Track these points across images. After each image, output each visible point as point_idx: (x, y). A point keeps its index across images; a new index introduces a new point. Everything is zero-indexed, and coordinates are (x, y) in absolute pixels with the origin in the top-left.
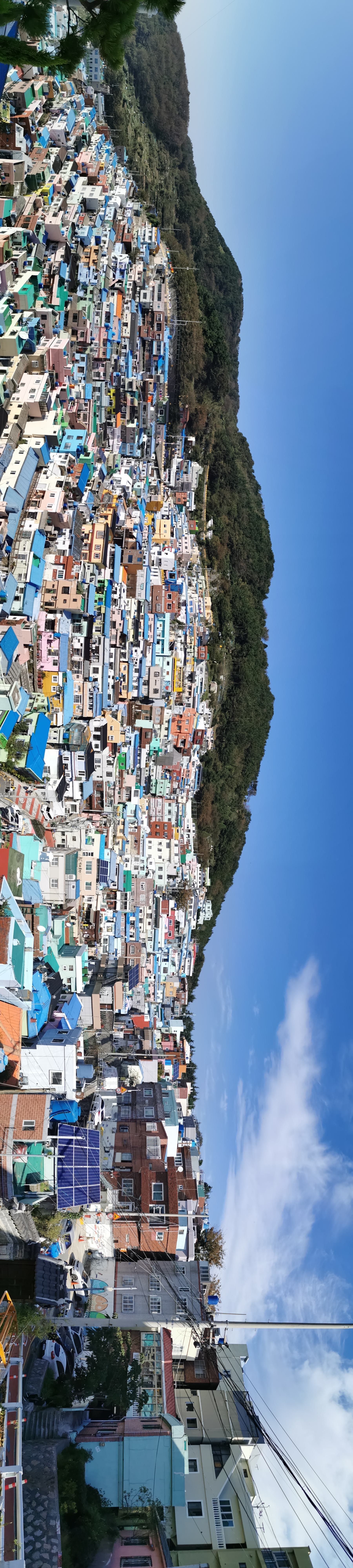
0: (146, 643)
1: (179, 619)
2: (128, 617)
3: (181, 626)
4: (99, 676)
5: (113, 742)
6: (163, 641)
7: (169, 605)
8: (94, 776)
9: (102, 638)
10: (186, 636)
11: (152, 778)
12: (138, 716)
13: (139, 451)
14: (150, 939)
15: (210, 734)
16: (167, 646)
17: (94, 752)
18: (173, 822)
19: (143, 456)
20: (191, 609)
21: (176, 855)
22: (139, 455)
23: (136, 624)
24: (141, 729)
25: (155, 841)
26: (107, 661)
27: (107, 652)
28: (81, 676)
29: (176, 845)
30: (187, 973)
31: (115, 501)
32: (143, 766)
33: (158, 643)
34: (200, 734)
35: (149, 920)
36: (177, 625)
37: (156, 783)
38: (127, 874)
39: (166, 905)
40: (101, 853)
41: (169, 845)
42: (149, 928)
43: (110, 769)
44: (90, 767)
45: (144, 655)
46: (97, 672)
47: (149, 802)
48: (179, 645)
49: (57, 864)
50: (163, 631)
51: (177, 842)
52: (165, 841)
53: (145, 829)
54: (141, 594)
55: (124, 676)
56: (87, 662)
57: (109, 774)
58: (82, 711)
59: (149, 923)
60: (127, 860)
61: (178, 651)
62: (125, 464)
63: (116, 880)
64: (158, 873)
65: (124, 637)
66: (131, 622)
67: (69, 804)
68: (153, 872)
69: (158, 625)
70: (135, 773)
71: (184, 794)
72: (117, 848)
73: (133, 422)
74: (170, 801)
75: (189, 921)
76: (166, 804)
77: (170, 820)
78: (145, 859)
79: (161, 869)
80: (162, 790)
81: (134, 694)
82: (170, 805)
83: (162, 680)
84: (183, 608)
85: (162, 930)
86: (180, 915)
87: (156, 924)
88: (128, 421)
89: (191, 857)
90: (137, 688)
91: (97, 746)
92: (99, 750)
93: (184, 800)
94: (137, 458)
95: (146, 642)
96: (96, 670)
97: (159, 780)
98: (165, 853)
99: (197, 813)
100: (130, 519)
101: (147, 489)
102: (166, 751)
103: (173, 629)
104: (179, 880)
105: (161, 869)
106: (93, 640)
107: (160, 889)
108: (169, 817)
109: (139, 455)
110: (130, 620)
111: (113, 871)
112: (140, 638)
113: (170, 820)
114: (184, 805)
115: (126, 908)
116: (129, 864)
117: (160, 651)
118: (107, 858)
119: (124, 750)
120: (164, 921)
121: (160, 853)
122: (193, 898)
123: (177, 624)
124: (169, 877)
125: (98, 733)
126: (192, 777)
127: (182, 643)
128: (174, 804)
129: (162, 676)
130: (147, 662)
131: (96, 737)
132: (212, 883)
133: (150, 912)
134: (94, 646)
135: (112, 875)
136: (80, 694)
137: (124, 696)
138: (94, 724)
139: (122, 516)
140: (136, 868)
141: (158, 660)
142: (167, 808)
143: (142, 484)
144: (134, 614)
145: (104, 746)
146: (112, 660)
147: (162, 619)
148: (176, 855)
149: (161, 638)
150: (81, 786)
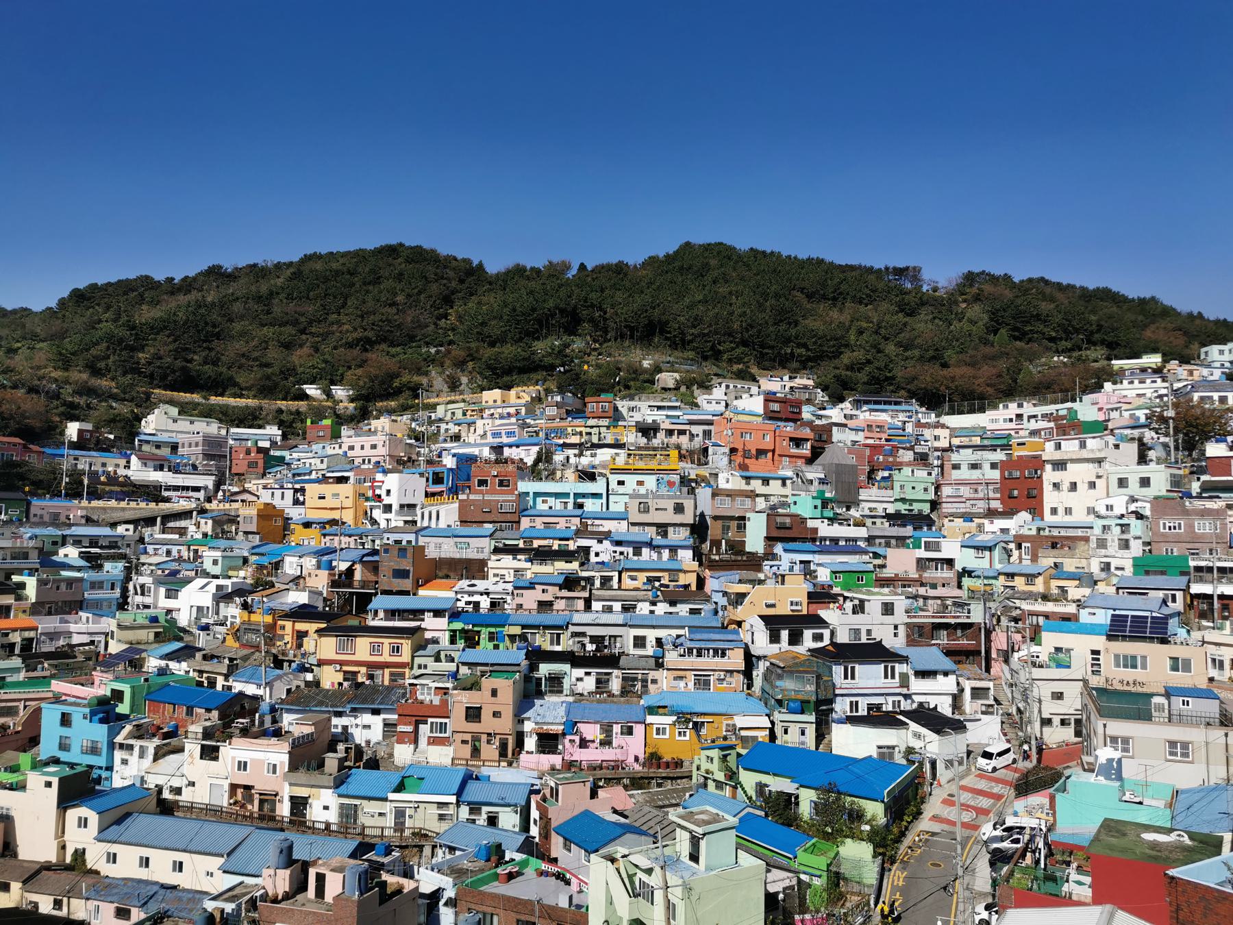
0: (581, 532)
1: (529, 461)
2: (529, 575)
3: (545, 457)
4: (651, 635)
5: (805, 601)
7: (501, 484)
8: (895, 643)
10: (565, 446)
11: (891, 509)
13: (108, 566)
16: (588, 487)
17: (833, 643)
18: (999, 456)
19: (123, 557)
20: (510, 434)
21: (1083, 445)
22: (121, 565)
23: (543, 555)
25: (1050, 498)
26: (619, 618)
27: (600, 618)
28: (652, 675)
29: (1058, 447)
31: (254, 618)
32: (862, 532)
33: (581, 506)
36: (542, 467)
37: (903, 500)
41: (1060, 465)
45: (607, 535)
46: (643, 638)
47: (955, 515)
48: (585, 461)
49: (1126, 741)
50: (557, 495)
51: (1050, 446)
52: (1049, 475)
53: (1021, 523)
54: (478, 547)
58: (731, 672)
61: (596, 461)
62: (148, 600)
64: (1134, 488)
65: (570, 583)
66: (538, 568)
67: (969, 705)
68: (1133, 500)
69: (545, 507)
70: (880, 551)
71: (928, 433)
73: (22, 586)
74: (947, 466)
76: (956, 474)
77: (994, 466)
79: (1122, 483)
80: (920, 487)
81: (686, 556)
82: (956, 467)
84: (507, 452)
88: (19, 598)
90: (673, 550)
91: (818, 638)
92: (826, 633)
94: (128, 570)
95: (579, 533)
96: (640, 642)
97: (897, 493)
100: (305, 576)
101: (223, 543)
103: (551, 476)
104: (1149, 435)
105: (1122, 483)
106: (576, 648)
107: (1176, 482)
108: (987, 466)
109: (121, 565)
112: (572, 546)
113: (994, 466)
117: (598, 502)
119: (823, 575)
123: (541, 466)
124: (1143, 459)
125: (785, 634)
127: (581, 455)
130: (619, 528)
131: (795, 639)
134: (590, 647)
137: (691, 579)
138: (761, 643)
139: (298, 598)
140: (1125, 545)
141: (617, 506)
142: (965, 473)
143: (209, 556)
144: (521, 562)
145: (815, 621)
146: (617, 606)
147: (530, 499)
148: (1083, 445)
149: (571, 500)
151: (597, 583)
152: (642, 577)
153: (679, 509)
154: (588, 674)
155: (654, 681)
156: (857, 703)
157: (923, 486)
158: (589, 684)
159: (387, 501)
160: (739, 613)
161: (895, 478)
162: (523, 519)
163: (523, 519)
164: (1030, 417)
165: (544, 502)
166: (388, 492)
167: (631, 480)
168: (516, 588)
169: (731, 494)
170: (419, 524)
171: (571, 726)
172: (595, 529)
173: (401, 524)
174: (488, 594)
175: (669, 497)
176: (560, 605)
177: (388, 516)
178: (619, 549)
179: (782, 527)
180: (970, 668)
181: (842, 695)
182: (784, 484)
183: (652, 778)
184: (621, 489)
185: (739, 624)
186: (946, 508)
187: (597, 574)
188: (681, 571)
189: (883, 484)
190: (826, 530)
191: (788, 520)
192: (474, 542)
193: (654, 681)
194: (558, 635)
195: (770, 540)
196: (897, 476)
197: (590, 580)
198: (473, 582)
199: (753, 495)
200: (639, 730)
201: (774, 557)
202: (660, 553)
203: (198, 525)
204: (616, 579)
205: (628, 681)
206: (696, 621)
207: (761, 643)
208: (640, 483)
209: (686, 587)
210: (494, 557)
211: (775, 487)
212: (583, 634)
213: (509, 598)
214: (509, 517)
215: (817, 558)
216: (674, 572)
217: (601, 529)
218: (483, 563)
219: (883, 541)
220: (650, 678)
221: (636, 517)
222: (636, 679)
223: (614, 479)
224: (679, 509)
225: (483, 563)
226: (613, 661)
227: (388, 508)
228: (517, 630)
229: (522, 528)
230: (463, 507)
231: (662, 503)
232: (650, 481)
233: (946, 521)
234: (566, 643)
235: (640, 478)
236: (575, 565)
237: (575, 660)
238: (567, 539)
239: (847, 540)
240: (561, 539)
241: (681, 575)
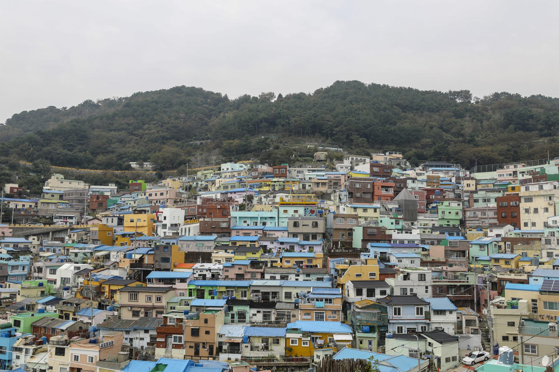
34: (376, 169)
37: (443, 219)
46: (290, 293)
56: (278, 306)
58: (335, 312)
70: (427, 247)
76: (476, 205)
82: (476, 201)
138: (352, 296)
142: (481, 205)
146: (278, 277)
149: (259, 221)
151: (269, 265)
152: (293, 262)
153: (316, 225)
154: (259, 312)
155: (294, 316)
156: (402, 327)
157: (455, 211)
158: (259, 318)
159: (164, 222)
161: (439, 207)
164: (520, 173)
165: (245, 222)
166: (165, 218)
167: (291, 210)
169: (344, 217)
170: (180, 234)
173: (171, 234)
177: (164, 230)
178: (282, 246)
181: (393, 323)
184: (285, 215)
186: (468, 224)
189: (433, 211)
191: (375, 231)
192: (206, 244)
193: (294, 316)
194: (245, 292)
195: (365, 241)
196: (441, 208)
197: (265, 263)
198: (203, 264)
199: (356, 217)
200: (282, 342)
201: (367, 250)
203: (70, 236)
205: (280, 315)
207: (352, 296)
208: (296, 211)
210: (215, 251)
212: (258, 291)
214: (225, 231)
215: (389, 251)
217: (274, 236)
219: (429, 241)
220: (292, 314)
223: (282, 209)
226: (272, 305)
227: (164, 226)
230: (202, 225)
231: (306, 222)
232: (301, 210)
233: (467, 230)
234: (250, 296)
235: (296, 209)
236: (257, 256)
237: (252, 304)
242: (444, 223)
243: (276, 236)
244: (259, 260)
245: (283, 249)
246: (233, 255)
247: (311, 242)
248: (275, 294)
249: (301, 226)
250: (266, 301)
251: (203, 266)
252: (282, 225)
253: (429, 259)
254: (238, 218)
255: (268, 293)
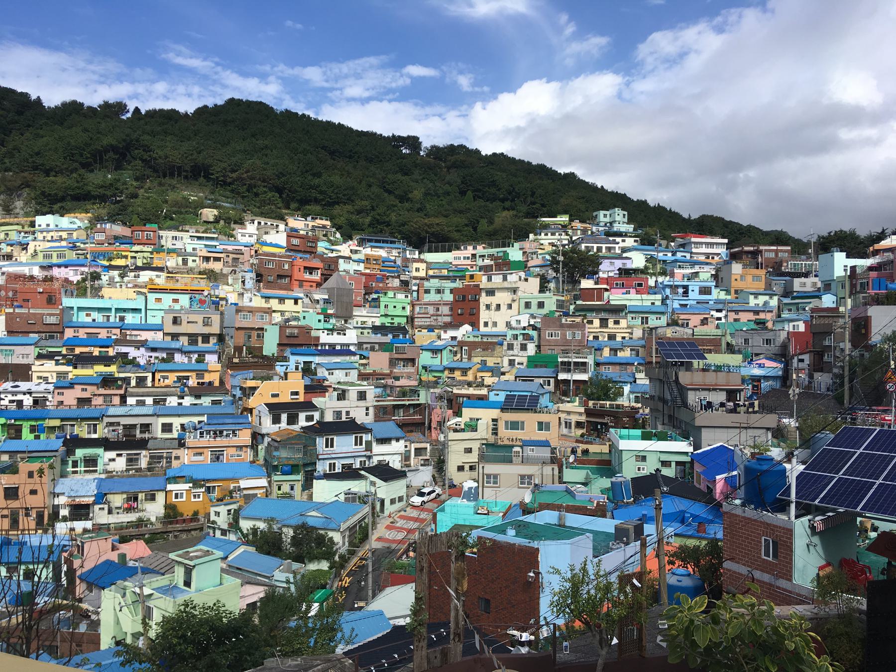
0: (123, 341)
4: (176, 422)
5: (302, 391)
6: (117, 310)
9: (106, 420)
11: (378, 323)
12: (256, 352)
14: (645, 321)
15: (298, 223)
21: (505, 279)
24: (279, 345)
25: (484, 316)
27: (133, 410)
28: (175, 453)
29: (490, 279)
30: (723, 251)
33: (122, 319)
34: (295, 241)
35: (611, 323)
37: (386, 315)
38: (533, 362)
39: (588, 294)
40: (492, 406)
41: (491, 292)
42: (623, 323)
43: (353, 394)
44: (349, 427)
46: (171, 425)
47: (420, 327)
50: (100, 310)
52: (484, 299)
53: (464, 331)
55: (179, 379)
57: (362, 396)
58: (240, 448)
59: (617, 322)
60: (512, 363)
63: (541, 381)
64: (534, 309)
65: (107, 381)
69: (89, 320)
70: (365, 353)
72: (489, 380)
75: (624, 250)
78: (510, 333)
79: (528, 305)
80: (399, 306)
83: (190, 312)
85: (633, 299)
86: (608, 269)
87: (618, 310)
89: (515, 253)
93: (422, 266)
95: (118, 342)
96: (167, 428)
97: (382, 310)
98: (502, 298)
99: (444, 243)
102: (326, 301)
105: (528, 305)
107: (560, 305)
110: (73, 373)
111: (527, 386)
112: (111, 352)
114: (430, 266)
115: (584, 364)
116: (518, 360)
117: (138, 316)
118: (502, 397)
120: (616, 298)
121: (504, 308)
122: (583, 246)
124: (543, 289)
125: (284, 417)
126: (382, 253)
128: (426, 284)
129: (179, 311)
131: (292, 420)
132: (565, 212)
133: (597, 322)
135: (524, 389)
136: (208, 454)
141: (155, 319)
145: (308, 406)
146: (149, 401)
148: (505, 279)
150: (383, 441)
154: (119, 455)
155: (177, 458)
158: (120, 464)
160: (252, 402)
162: (67, 330)
163: (67, 330)
165: (87, 315)
167: (167, 299)
168: (56, 388)
169: (252, 311)
171: (101, 498)
172: (133, 338)
174: (30, 393)
175: (198, 313)
176: (98, 401)
178: (154, 354)
179: (292, 336)
180: (417, 435)
182: (296, 303)
183: (170, 532)
185: (251, 411)
187: (133, 375)
188: (206, 371)
189: (372, 304)
190: (325, 338)
191: (296, 331)
192: (19, 350)
193: (177, 458)
194: (95, 425)
197: (127, 380)
198: (17, 383)
200: (160, 497)
202: (190, 358)
204: (150, 379)
206: (217, 410)
208: (176, 301)
209: (210, 383)
210: (37, 363)
211: (289, 305)
212: (118, 424)
213: (50, 397)
214: (54, 328)
216: (200, 374)
217: (139, 338)
218: (28, 367)
220: (173, 455)
221: (170, 328)
222: (161, 457)
223: (152, 297)
224: (207, 323)
225: (28, 367)
226: (143, 444)
228: (57, 423)
229: (65, 338)
231: (192, 318)
232: (184, 300)
234: (102, 432)
235: (175, 296)
236: (113, 369)
238: (108, 347)
239: (342, 345)
240: (101, 347)
241: (206, 375)
242: (387, 321)
243: (143, 338)
244: (117, 375)
245: (157, 358)
246: (70, 368)
247: (201, 346)
248: (146, 427)
249: (184, 323)
250: (130, 441)
251: (17, 386)
252: (151, 321)
253: (369, 370)
254: (75, 309)
255: (134, 426)
